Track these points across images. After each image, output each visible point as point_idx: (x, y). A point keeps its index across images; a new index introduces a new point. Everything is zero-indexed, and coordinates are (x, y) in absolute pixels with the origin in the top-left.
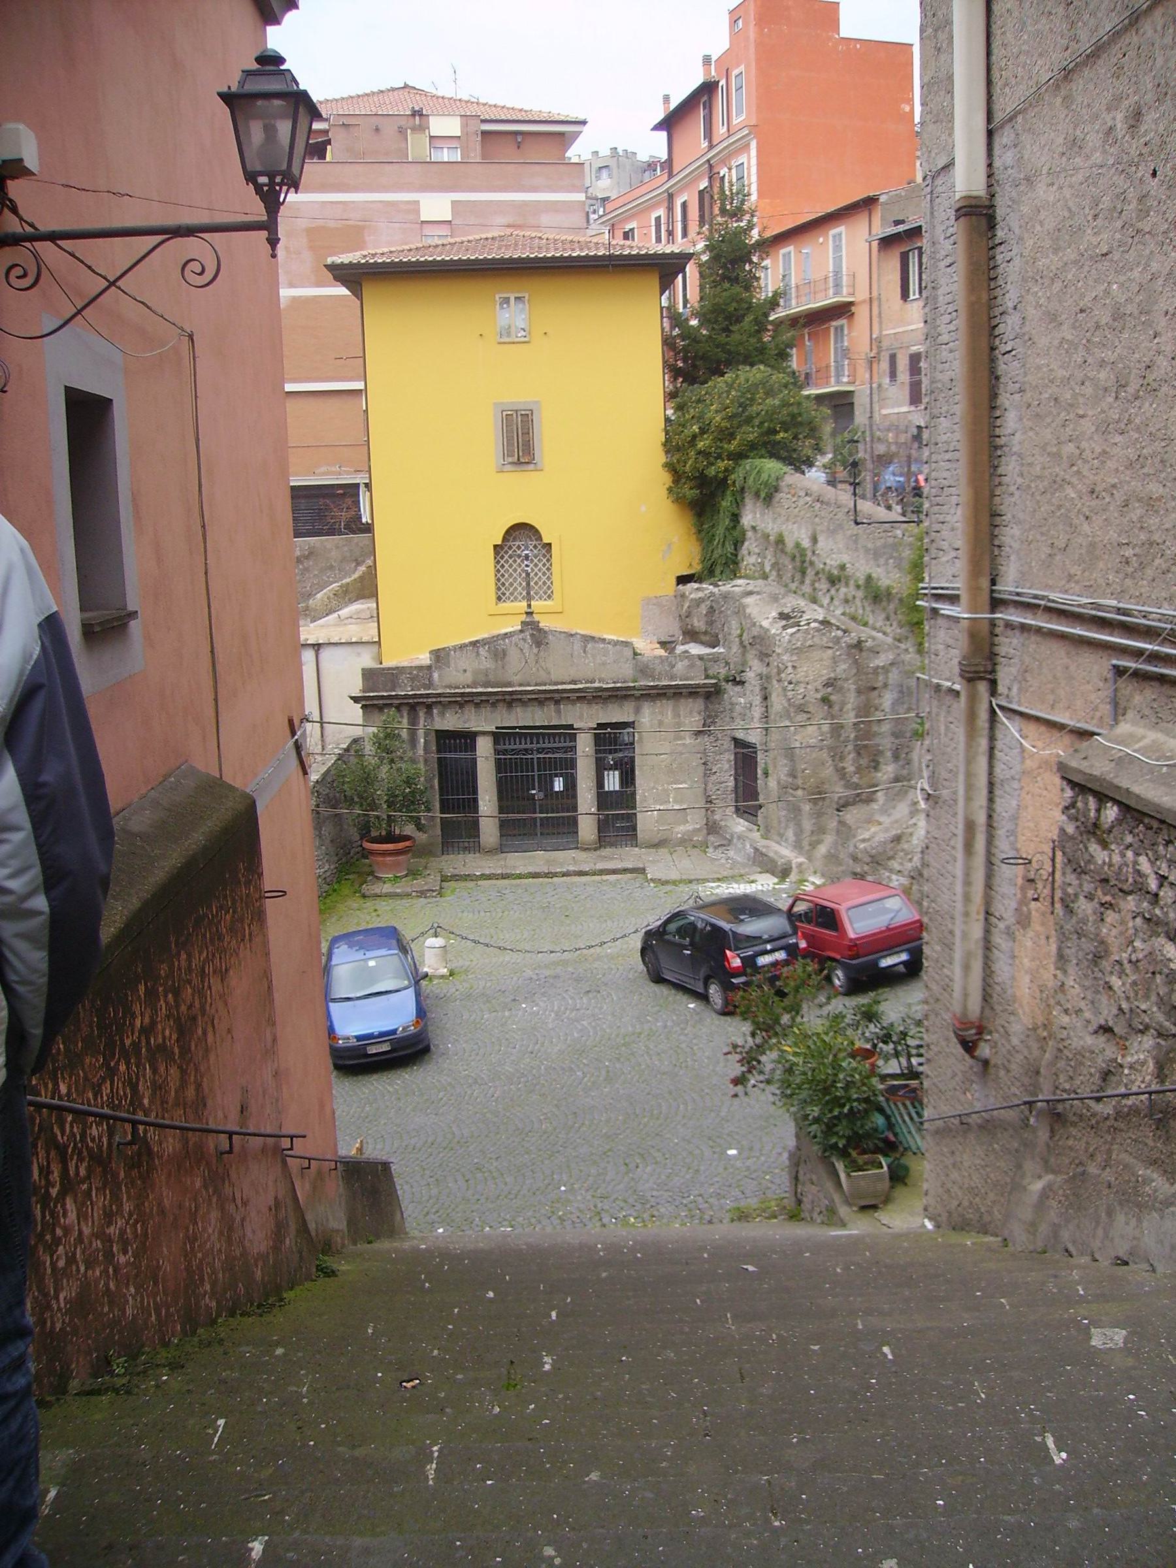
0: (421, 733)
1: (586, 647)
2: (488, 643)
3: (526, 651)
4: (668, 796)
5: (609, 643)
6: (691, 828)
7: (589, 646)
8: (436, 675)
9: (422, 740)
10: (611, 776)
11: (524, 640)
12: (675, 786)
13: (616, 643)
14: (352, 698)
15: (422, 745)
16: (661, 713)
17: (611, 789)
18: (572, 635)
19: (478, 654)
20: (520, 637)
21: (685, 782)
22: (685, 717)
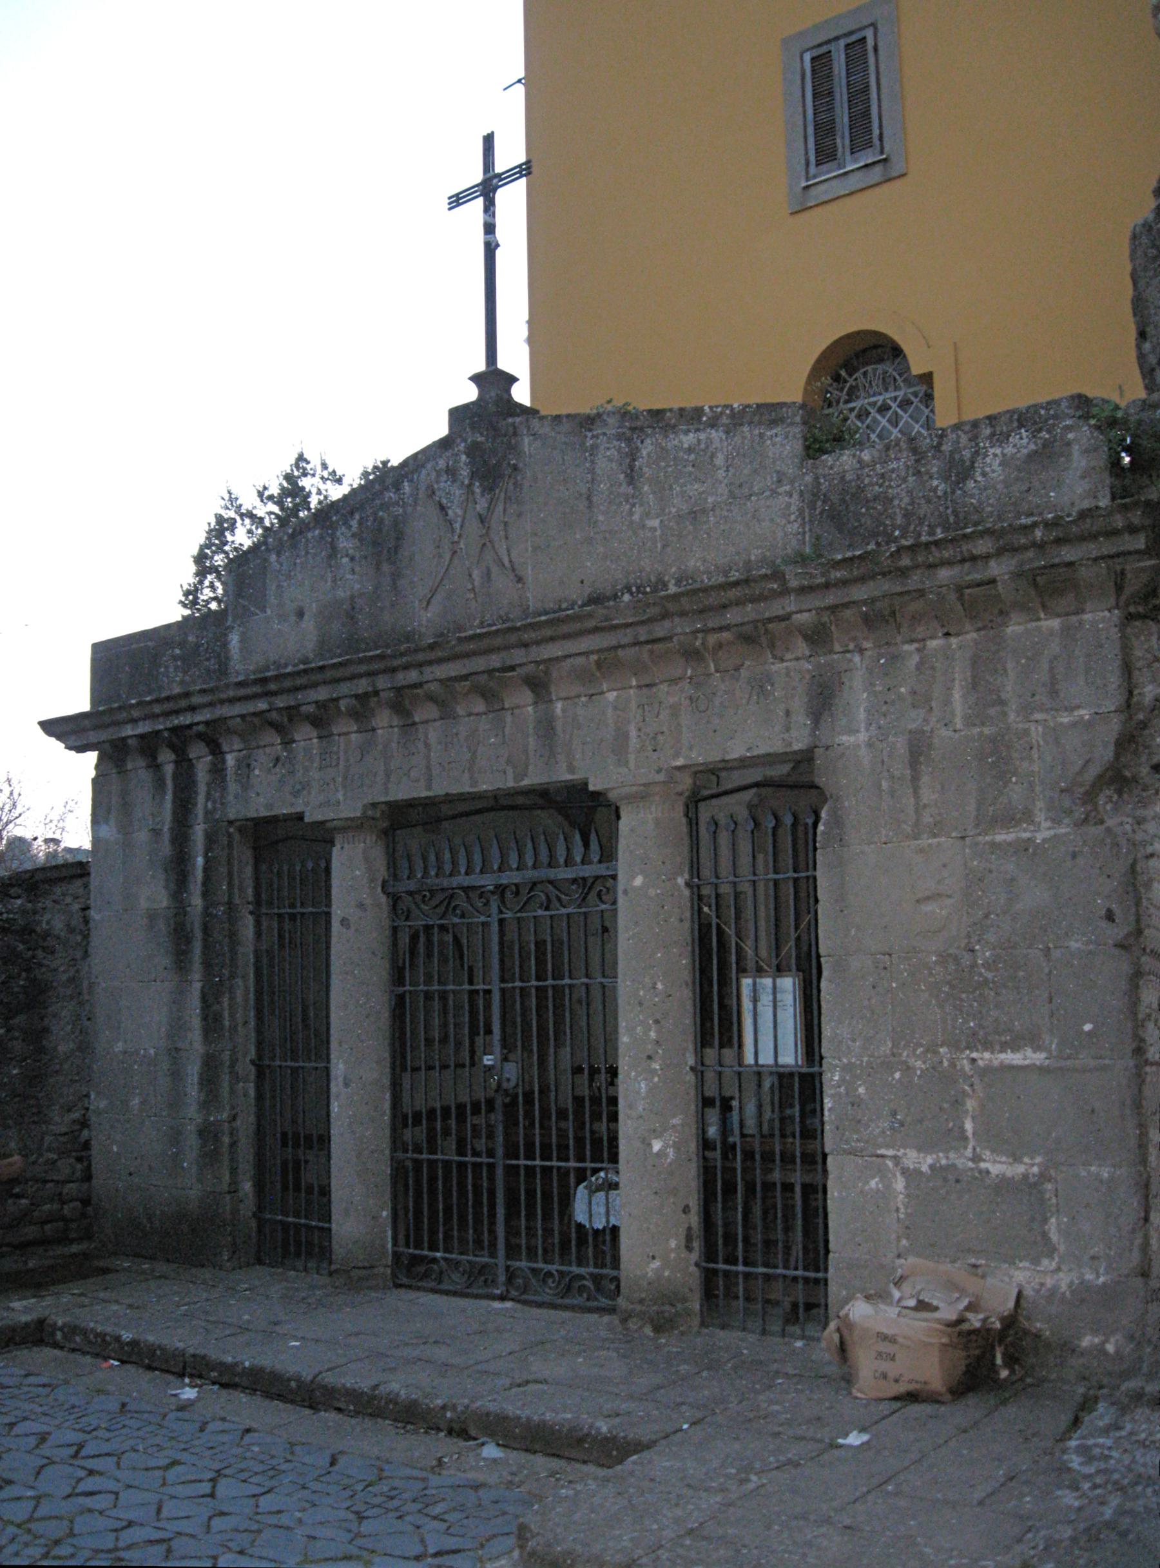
0: (199, 832)
1: (633, 455)
2: (361, 507)
3: (455, 511)
4: (957, 1103)
5: (713, 424)
6: (1064, 1280)
7: (647, 448)
8: (234, 639)
9: (200, 861)
10: (766, 999)
11: (451, 472)
12: (985, 1057)
13: (738, 418)
14: (51, 727)
15: (199, 874)
16: (921, 700)
17: (766, 1059)
18: (588, 422)
19: (334, 551)
20: (442, 464)
21: (1032, 1039)
22: (1026, 710)
